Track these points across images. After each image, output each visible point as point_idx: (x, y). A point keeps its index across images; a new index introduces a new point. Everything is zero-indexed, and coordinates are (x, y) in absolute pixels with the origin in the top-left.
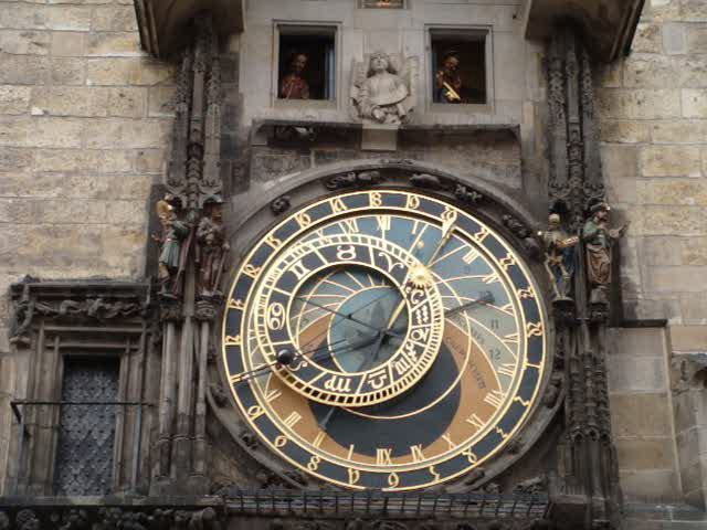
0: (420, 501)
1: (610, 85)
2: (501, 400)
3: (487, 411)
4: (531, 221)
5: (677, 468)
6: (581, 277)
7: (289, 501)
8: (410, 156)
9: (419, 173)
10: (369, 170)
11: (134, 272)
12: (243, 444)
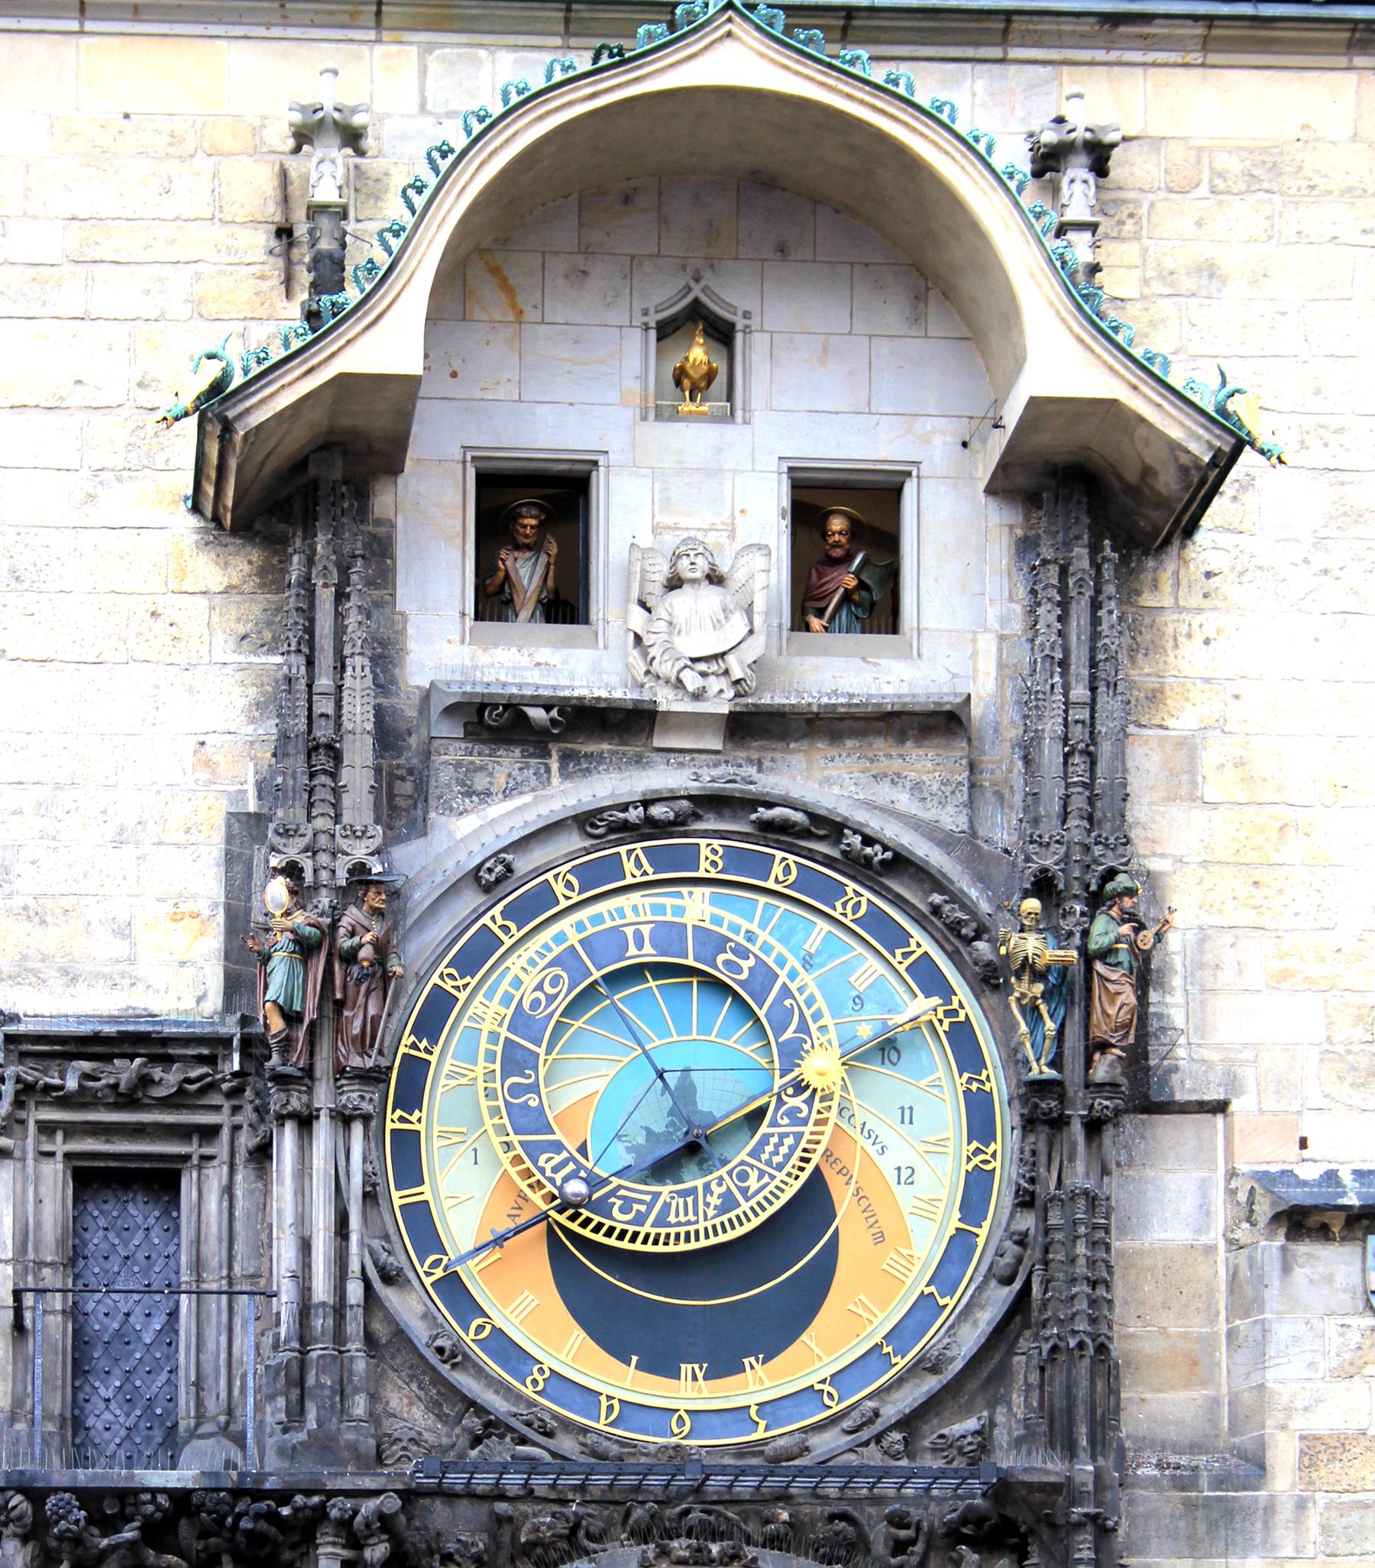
1: (1148, 600)
4: (985, 907)
5: (1224, 1389)
6: (1076, 1028)
8: (750, 761)
9: (769, 805)
11: (198, 1002)
12: (434, 1359)
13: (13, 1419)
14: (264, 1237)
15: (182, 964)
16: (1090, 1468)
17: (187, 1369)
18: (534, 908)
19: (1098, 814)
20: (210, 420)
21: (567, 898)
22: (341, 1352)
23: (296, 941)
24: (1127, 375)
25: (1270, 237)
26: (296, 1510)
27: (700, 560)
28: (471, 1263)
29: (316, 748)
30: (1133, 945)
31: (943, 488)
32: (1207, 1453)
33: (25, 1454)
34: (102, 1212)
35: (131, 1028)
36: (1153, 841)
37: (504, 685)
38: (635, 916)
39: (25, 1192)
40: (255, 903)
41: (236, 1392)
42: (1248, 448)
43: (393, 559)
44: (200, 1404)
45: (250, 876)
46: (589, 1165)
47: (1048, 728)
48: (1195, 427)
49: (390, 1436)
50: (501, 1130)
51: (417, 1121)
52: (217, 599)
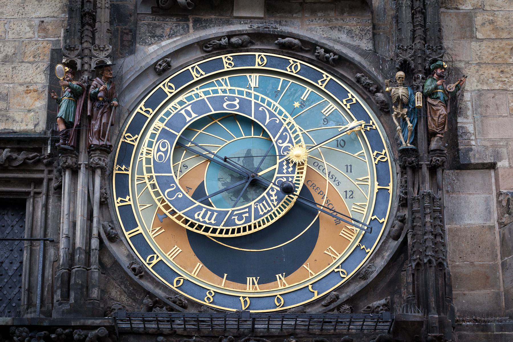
0: (282, 321)
7: (171, 321)
8: (276, 22)
9: (283, 37)
10: (239, 34)
11: (36, 125)
19: (428, 37)
22: (88, 270)
36: (456, 55)
49: (110, 308)
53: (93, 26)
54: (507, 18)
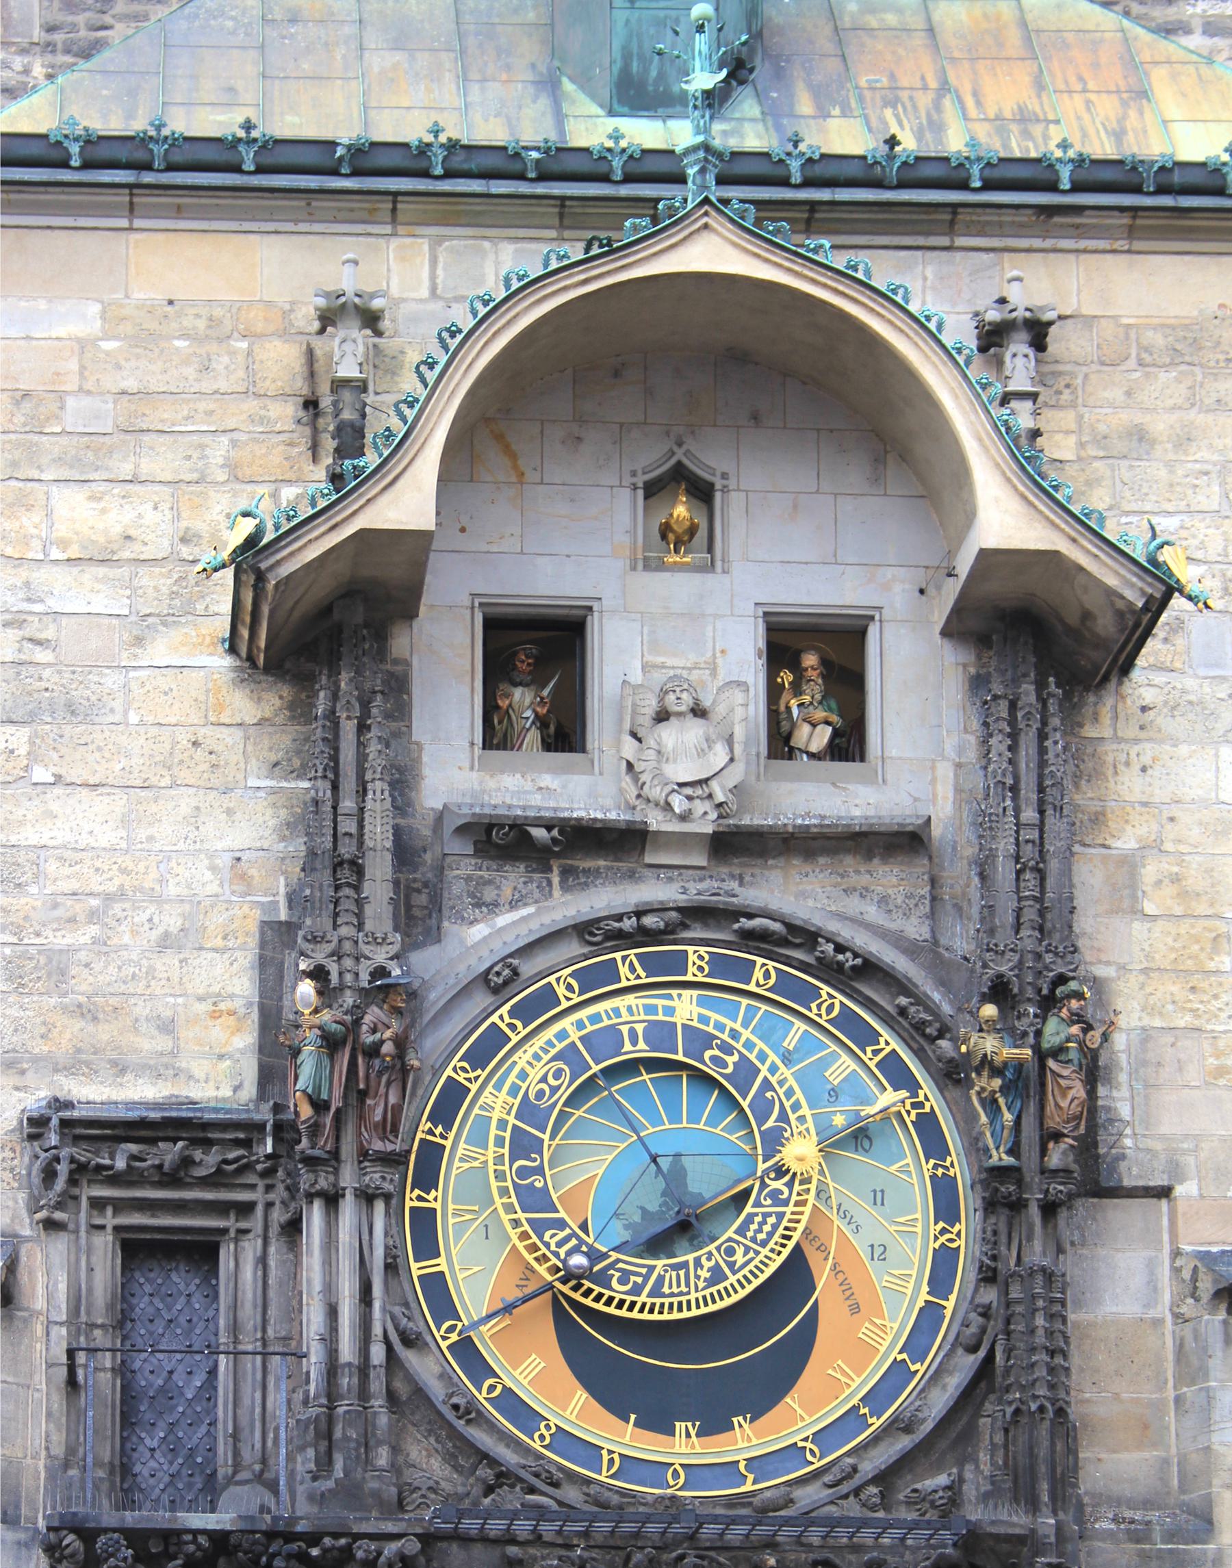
1: (1089, 731)
2: (887, 1334)
3: (863, 1353)
4: (947, 1009)
8: (732, 876)
9: (750, 916)
10: (661, 909)
12: (450, 1415)
13: (66, 1465)
14: (295, 1303)
15: (221, 1057)
16: (1052, 1521)
17: (225, 1422)
18: (538, 1007)
20: (245, 571)
21: (568, 999)
23: (323, 1037)
24: (1067, 529)
25: (1193, 405)
26: (325, 1551)
27: (685, 696)
28: (483, 1328)
29: (341, 864)
30: (1082, 1044)
31: (903, 631)
32: (1159, 1509)
33: (78, 1497)
34: (147, 1280)
35: (174, 1114)
37: (510, 807)
38: (628, 1013)
39: (78, 1261)
40: (286, 1003)
41: (270, 1443)
42: (1176, 594)
43: (409, 694)
44: (236, 1453)
45: (282, 977)
46: (590, 1241)
47: (1001, 846)
48: (1129, 576)
50: (509, 1208)
51: (434, 1200)
52: (251, 730)
53: (357, 888)
54: (1209, 871)
